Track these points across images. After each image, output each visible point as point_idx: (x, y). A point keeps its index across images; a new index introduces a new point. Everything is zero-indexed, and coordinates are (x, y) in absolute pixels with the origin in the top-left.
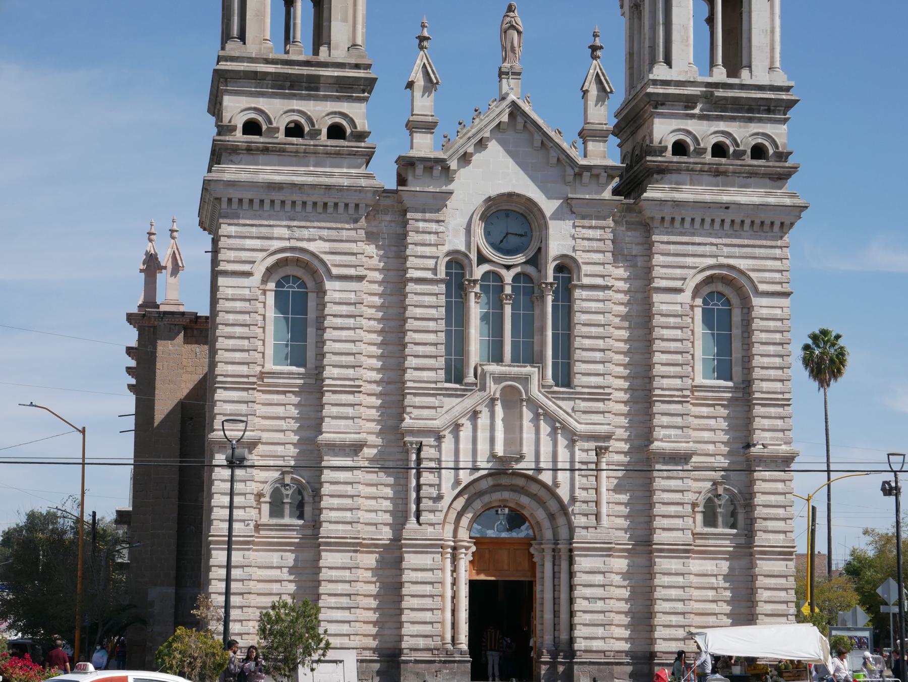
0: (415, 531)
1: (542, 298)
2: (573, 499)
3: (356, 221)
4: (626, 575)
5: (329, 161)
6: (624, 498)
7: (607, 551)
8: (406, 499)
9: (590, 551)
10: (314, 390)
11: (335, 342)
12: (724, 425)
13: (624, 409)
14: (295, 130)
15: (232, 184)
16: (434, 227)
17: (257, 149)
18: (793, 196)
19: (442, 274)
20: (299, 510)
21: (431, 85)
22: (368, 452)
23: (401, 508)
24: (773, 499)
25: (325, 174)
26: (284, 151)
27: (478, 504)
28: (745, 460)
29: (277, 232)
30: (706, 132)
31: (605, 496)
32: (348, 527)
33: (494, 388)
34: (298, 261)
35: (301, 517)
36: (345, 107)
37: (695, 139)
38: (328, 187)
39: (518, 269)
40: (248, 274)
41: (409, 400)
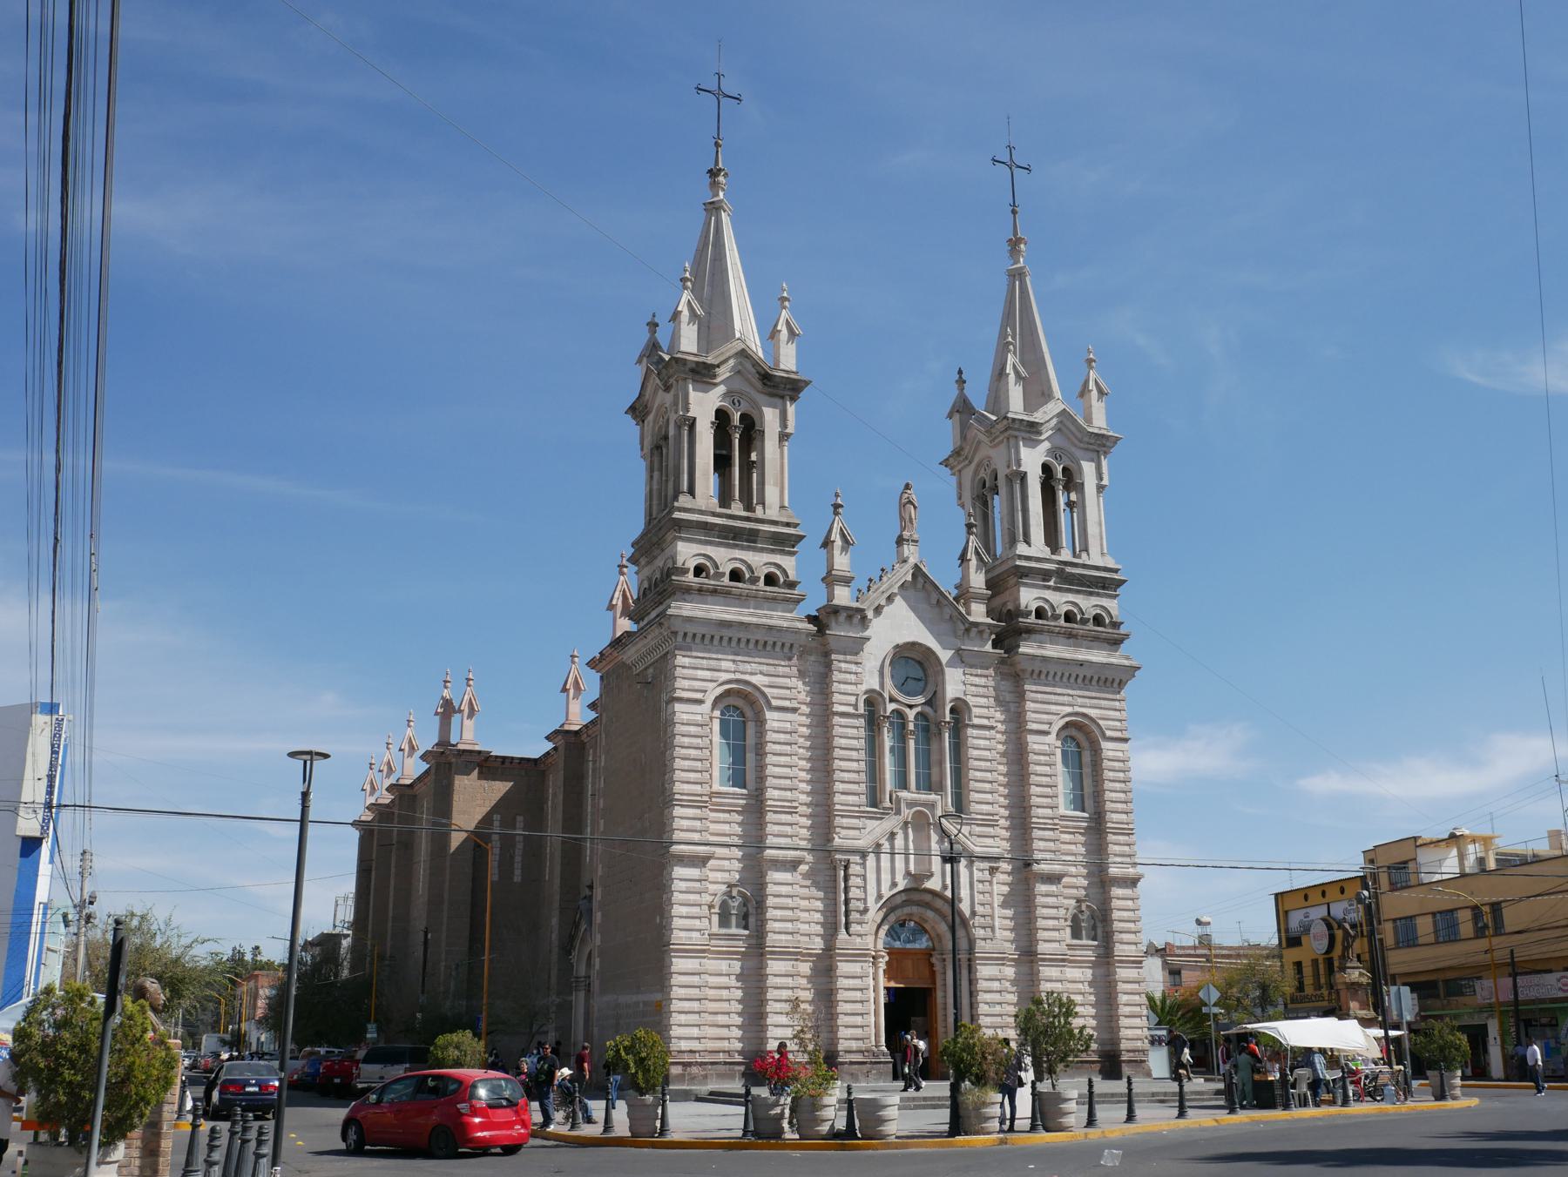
0: (846, 942)
1: (940, 734)
2: (974, 913)
3: (790, 659)
4: (1014, 982)
5: (766, 605)
6: (1009, 913)
7: (1001, 960)
8: (835, 913)
9: (988, 960)
10: (756, 810)
11: (775, 766)
12: (1082, 850)
13: (1006, 834)
14: (736, 575)
15: (689, 619)
16: (853, 668)
17: (707, 590)
18: (1127, 658)
19: (861, 710)
20: (744, 921)
21: (847, 543)
22: (804, 868)
23: (830, 920)
24: (1125, 914)
25: (766, 616)
26: (729, 593)
27: (892, 918)
28: (1101, 881)
29: (725, 665)
30: (1061, 601)
31: (998, 911)
32: (789, 937)
33: (907, 813)
34: (738, 693)
35: (746, 928)
36: (778, 559)
37: (1052, 606)
38: (771, 628)
39: (919, 709)
40: (700, 702)
41: (838, 821)
